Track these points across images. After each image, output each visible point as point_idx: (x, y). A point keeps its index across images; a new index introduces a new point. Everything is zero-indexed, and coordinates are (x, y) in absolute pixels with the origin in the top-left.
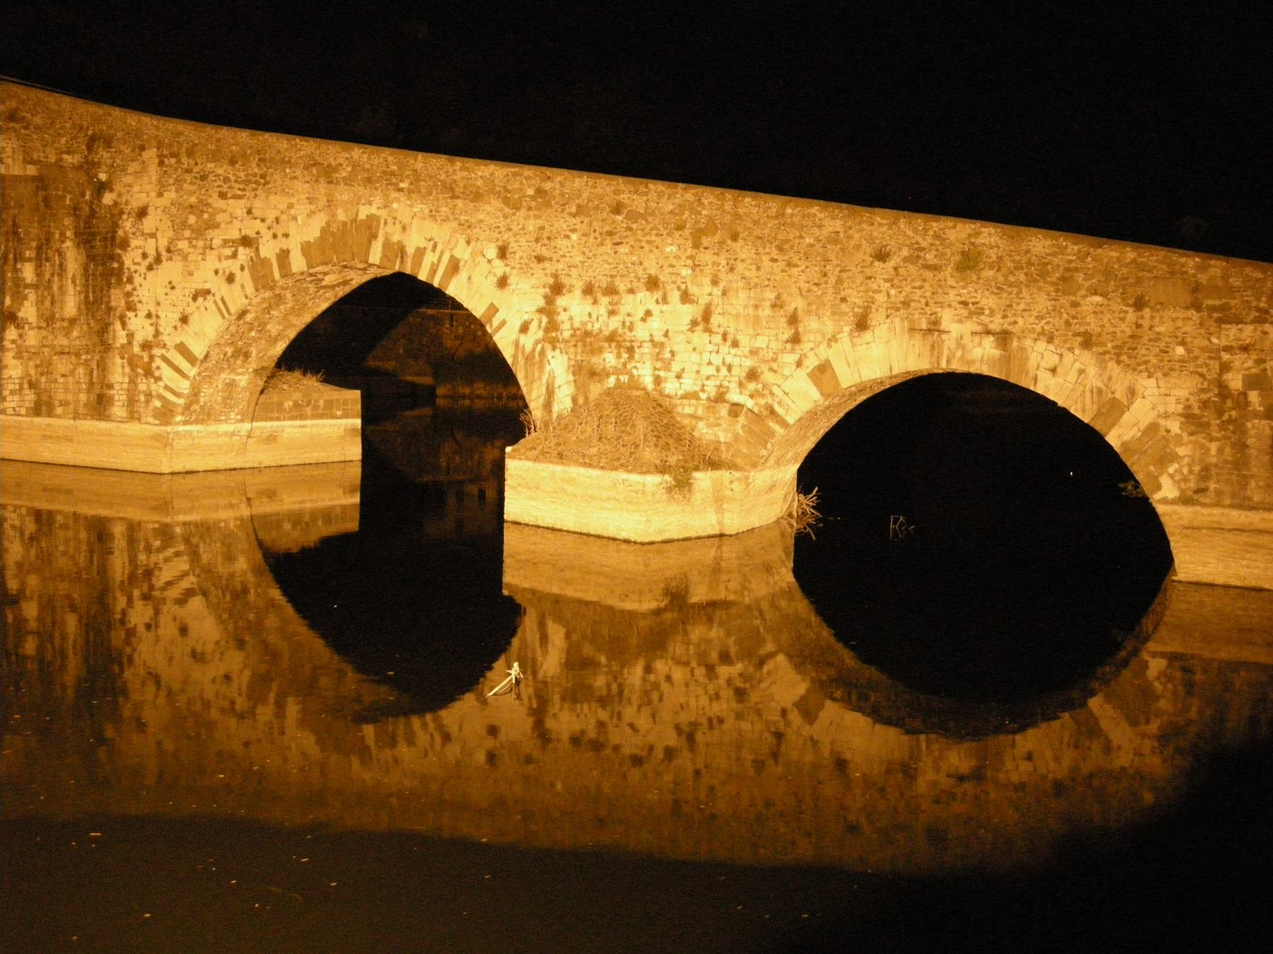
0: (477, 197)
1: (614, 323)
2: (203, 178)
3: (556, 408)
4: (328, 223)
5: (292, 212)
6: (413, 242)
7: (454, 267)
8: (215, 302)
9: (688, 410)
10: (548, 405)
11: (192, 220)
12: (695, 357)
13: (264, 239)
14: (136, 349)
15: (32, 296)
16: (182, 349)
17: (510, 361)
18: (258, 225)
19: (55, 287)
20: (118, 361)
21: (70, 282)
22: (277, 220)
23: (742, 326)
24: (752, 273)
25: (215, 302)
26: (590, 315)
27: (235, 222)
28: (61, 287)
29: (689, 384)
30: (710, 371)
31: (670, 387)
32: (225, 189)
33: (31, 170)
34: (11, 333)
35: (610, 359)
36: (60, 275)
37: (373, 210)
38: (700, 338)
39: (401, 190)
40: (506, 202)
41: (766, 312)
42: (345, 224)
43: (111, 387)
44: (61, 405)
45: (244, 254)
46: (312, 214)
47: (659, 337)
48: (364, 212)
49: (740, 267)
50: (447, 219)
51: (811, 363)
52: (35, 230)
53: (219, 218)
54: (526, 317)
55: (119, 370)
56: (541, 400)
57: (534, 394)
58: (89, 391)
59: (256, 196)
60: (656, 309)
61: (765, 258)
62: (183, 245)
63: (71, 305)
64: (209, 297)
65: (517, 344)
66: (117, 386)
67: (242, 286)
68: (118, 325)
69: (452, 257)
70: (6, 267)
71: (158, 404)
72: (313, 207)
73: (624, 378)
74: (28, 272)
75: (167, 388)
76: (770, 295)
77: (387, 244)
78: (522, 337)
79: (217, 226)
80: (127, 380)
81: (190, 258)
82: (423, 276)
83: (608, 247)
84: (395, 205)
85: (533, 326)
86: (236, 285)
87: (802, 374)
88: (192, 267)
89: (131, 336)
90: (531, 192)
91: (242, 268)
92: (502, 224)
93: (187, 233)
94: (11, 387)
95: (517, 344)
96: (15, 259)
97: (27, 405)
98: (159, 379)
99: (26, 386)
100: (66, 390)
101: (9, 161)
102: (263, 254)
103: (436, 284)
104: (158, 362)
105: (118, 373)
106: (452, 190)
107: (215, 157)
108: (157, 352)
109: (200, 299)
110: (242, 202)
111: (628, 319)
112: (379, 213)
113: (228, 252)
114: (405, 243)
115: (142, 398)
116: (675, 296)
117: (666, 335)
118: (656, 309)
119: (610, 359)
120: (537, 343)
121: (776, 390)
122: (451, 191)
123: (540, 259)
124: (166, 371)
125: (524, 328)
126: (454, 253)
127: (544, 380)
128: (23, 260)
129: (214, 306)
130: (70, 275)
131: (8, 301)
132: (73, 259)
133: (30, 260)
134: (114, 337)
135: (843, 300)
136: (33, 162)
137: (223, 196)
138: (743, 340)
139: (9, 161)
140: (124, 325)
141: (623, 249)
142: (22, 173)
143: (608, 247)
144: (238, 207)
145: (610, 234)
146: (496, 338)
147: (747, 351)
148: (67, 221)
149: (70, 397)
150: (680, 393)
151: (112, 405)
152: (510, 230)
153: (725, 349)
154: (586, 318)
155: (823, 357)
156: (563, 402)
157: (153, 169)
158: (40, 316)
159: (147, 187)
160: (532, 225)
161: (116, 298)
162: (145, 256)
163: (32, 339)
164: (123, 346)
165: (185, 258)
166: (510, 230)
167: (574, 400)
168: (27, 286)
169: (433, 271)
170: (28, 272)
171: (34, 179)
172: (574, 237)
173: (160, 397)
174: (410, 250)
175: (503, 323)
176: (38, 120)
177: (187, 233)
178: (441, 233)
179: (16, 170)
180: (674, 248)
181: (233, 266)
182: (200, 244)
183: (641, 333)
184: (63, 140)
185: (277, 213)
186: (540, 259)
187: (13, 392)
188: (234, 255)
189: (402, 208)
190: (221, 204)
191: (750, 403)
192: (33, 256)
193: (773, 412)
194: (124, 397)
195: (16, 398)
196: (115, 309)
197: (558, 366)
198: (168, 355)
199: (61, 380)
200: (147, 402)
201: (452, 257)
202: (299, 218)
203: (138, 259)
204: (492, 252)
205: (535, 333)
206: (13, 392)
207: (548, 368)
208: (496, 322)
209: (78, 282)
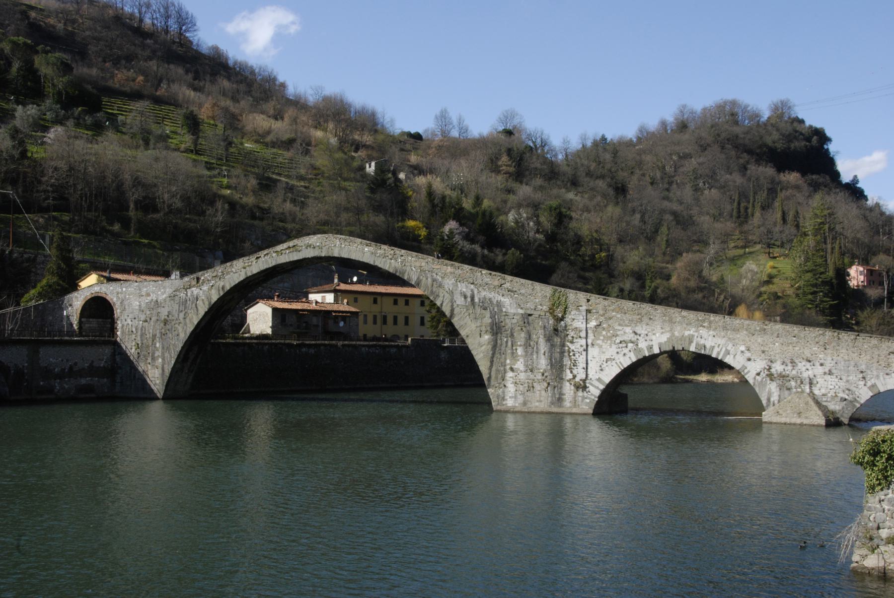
0: (736, 330)
1: (794, 372)
2: (610, 318)
3: (772, 399)
4: (671, 336)
5: (654, 332)
6: (708, 345)
7: (728, 353)
8: (616, 363)
9: (824, 399)
10: (769, 400)
11: (604, 333)
12: (826, 383)
13: (640, 342)
14: (577, 379)
15: (522, 360)
16: (599, 380)
17: (752, 384)
18: (638, 337)
19: (534, 357)
20: (568, 384)
21: (542, 355)
22: (647, 335)
23: (843, 373)
24: (846, 357)
25: (616, 363)
26: (784, 370)
27: (626, 334)
28: (537, 357)
29: (823, 391)
30: (832, 387)
31: (816, 392)
32: (622, 322)
33: (521, 311)
34: (510, 374)
35: (793, 383)
36: (537, 353)
37: (691, 332)
38: (828, 377)
39: (704, 327)
40: (750, 333)
41: (851, 368)
42: (677, 337)
43: (565, 395)
44: (538, 401)
45: (630, 345)
46: (662, 333)
47: (812, 376)
48: (687, 333)
49: (842, 355)
50: (724, 337)
51: (869, 384)
52: (523, 335)
53: (619, 333)
54: (758, 370)
55: (568, 388)
56: (766, 397)
57: (763, 395)
58: (552, 397)
59: (636, 326)
60: (810, 368)
61: (850, 352)
62: (599, 342)
63: (543, 363)
64: (614, 362)
65: (755, 378)
66: (567, 395)
67: (630, 358)
68: (568, 371)
69: (726, 350)
70: (507, 349)
71: (588, 401)
72: (663, 331)
73: (799, 390)
74: (520, 351)
75: (592, 394)
76: (852, 363)
77: (697, 344)
78: (757, 377)
79: (617, 335)
80: (572, 392)
81: (603, 347)
82: (714, 355)
83: (791, 347)
84: (701, 331)
85: (762, 373)
86: (627, 356)
87: (865, 388)
88: (604, 350)
89: (574, 377)
90: (758, 328)
91: (630, 351)
92: (747, 339)
93: (602, 338)
94: (511, 395)
95: (755, 378)
96: (512, 346)
97: (519, 402)
98: (589, 392)
99: (518, 395)
100: (540, 396)
101: (508, 307)
102: (640, 346)
103: (719, 358)
104: (588, 385)
105: (568, 390)
106: (726, 327)
107: (613, 311)
108: (587, 381)
109: (609, 362)
110: (630, 328)
111: (799, 371)
112: (694, 333)
113: (625, 345)
114: (706, 344)
115: (580, 398)
116: (818, 364)
117: (815, 376)
118: (810, 368)
119: (793, 383)
120: (763, 378)
121: (856, 393)
122: (725, 328)
123: (763, 352)
124: (591, 388)
125: (758, 374)
126: (728, 348)
127: (767, 390)
128: (517, 346)
129: (616, 365)
130: (543, 352)
131: (508, 361)
132: (543, 346)
133: (520, 346)
134: (566, 376)
135: (880, 365)
136: (522, 309)
137: (620, 325)
138: (844, 378)
139: (508, 307)
140: (571, 372)
141: (797, 348)
142: (515, 312)
143: (791, 347)
144: (628, 330)
145: (791, 343)
146: (746, 377)
147: (845, 381)
148: (541, 332)
149: (542, 399)
150: (821, 394)
151: (565, 401)
152: (750, 341)
153: (837, 380)
154: (782, 370)
155: (873, 382)
156: (775, 398)
157: (584, 313)
158: (526, 366)
159: (582, 321)
160: (760, 340)
161: (567, 362)
162: (581, 346)
163: (522, 376)
164: (570, 380)
165: (601, 347)
166: (750, 341)
167: (779, 396)
168: (519, 356)
169: (718, 353)
170: (520, 351)
171: (522, 314)
172: (777, 344)
173: (589, 398)
174: (708, 346)
175: (749, 372)
176: (523, 291)
177: (602, 338)
178: (721, 341)
179: (512, 311)
180: (816, 349)
181: (626, 351)
182: (609, 342)
183: (805, 375)
184: (537, 300)
185: (646, 332)
186: (763, 352)
187: (510, 397)
188: (626, 347)
189: (703, 332)
190: (620, 328)
191: (847, 397)
192: (523, 343)
193: (855, 399)
194: (571, 399)
195: (513, 399)
196: (566, 365)
197: (773, 387)
198: (593, 383)
199: (538, 392)
200: (582, 401)
201: (726, 350)
202: (657, 335)
203: (578, 346)
204: (743, 348)
205: (763, 375)
206: (510, 397)
207: (768, 387)
208: (746, 371)
209: (546, 354)
